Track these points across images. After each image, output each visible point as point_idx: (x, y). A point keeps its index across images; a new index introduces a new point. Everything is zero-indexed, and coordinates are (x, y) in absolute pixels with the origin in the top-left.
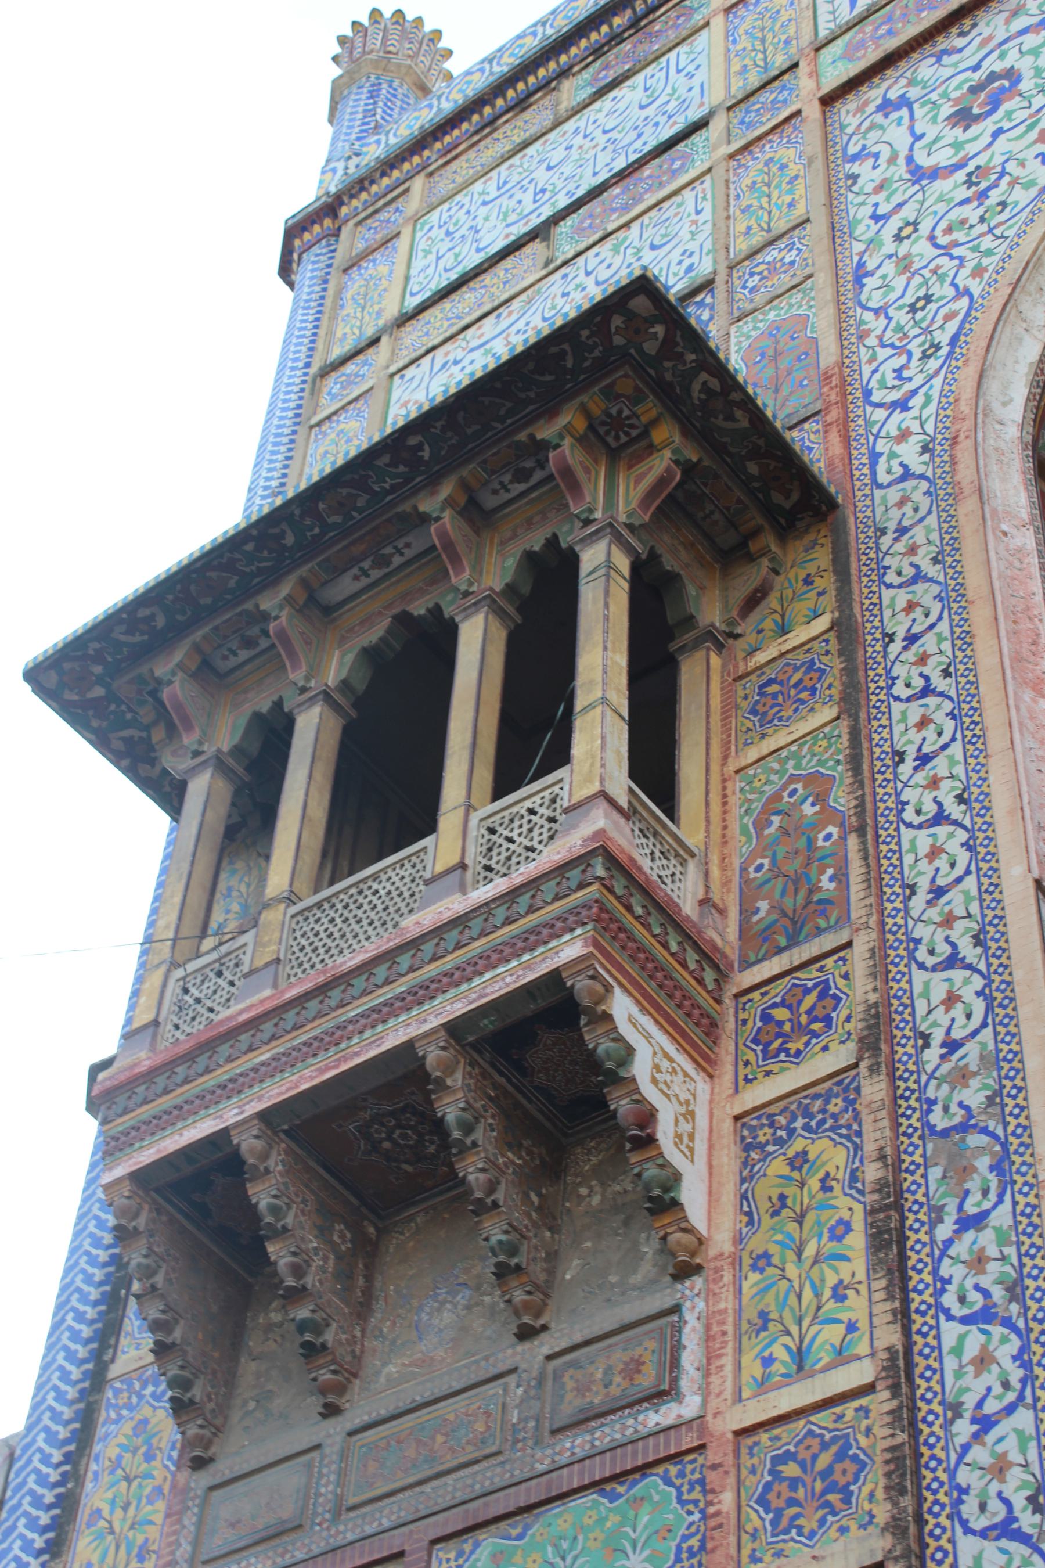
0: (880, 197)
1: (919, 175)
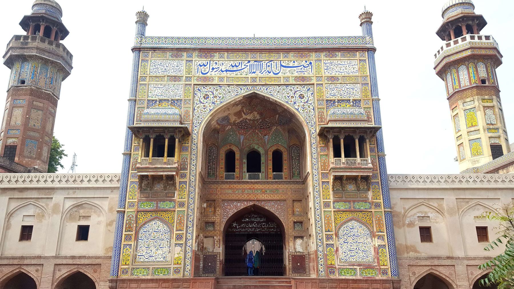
0: (197, 101)
1: (200, 102)
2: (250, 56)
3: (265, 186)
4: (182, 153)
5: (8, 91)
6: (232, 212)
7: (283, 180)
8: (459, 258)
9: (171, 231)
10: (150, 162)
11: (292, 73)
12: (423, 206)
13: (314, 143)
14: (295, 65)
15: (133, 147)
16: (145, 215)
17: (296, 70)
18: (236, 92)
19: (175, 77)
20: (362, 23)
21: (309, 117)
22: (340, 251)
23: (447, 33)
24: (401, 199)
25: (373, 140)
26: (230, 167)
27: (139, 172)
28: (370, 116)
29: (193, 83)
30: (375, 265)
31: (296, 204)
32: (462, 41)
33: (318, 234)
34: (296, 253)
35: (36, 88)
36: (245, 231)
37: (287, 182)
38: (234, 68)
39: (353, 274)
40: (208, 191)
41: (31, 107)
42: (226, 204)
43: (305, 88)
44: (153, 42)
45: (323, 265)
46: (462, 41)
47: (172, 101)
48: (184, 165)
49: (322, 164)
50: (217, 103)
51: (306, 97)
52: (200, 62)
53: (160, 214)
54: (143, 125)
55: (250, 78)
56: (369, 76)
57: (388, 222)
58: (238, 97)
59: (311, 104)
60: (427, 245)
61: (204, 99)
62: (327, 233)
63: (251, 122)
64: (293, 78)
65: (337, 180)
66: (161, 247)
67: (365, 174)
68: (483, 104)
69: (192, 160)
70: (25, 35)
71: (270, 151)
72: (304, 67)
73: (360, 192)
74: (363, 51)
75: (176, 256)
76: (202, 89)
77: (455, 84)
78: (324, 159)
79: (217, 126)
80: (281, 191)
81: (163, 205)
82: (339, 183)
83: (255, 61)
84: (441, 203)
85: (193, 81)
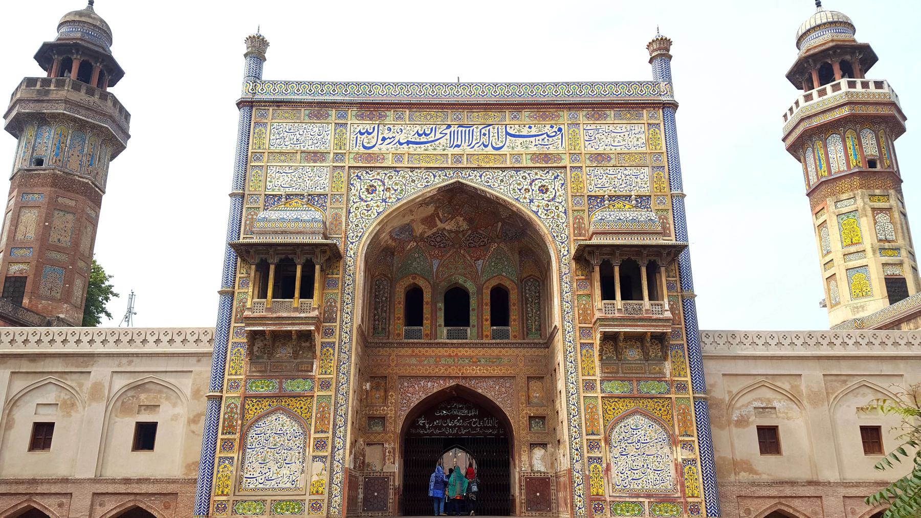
0: (354, 198)
1: (360, 198)
2: (451, 115)
3: (477, 351)
4: (327, 292)
5: (11, 179)
6: (417, 399)
7: (510, 341)
8: (829, 483)
9: (306, 434)
10: (268, 307)
11: (527, 147)
12: (764, 389)
13: (565, 274)
14: (531, 134)
15: (237, 279)
16: (258, 405)
17: (534, 142)
18: (425, 181)
19: (315, 153)
20: (653, 57)
21: (558, 226)
22: (614, 470)
23: (807, 76)
24: (724, 375)
25: (673, 268)
26: (414, 316)
27: (248, 325)
28: (668, 225)
29: (347, 164)
30: (676, 496)
31: (534, 385)
32: (834, 91)
33: (573, 439)
34: (532, 474)
35: (64, 172)
36: (440, 434)
37: (516, 343)
38: (421, 137)
39: (637, 512)
40: (373, 360)
41: (53, 206)
42: (406, 384)
43: (551, 174)
44: (277, 91)
45: (582, 496)
46: (834, 91)
47: (310, 197)
48: (331, 313)
49: (581, 312)
50: (390, 201)
51: (551, 190)
52: (361, 127)
53: (285, 402)
54: (256, 240)
55: (450, 156)
56: (665, 154)
57: (700, 417)
58: (429, 190)
59: (560, 203)
60: (771, 459)
61: (366, 193)
62: (589, 437)
63: (453, 235)
64: (529, 157)
65: (608, 341)
66: (286, 462)
67: (658, 331)
68: (871, 204)
69: (345, 304)
70: (45, 78)
71: (487, 287)
72: (548, 136)
73: (649, 362)
74: (654, 108)
75: (315, 478)
76: (364, 175)
77: (821, 169)
78: (584, 302)
79: (390, 242)
80: (505, 361)
81: (292, 386)
82: (612, 345)
83: (460, 126)
84: (796, 383)
85: (347, 160)
